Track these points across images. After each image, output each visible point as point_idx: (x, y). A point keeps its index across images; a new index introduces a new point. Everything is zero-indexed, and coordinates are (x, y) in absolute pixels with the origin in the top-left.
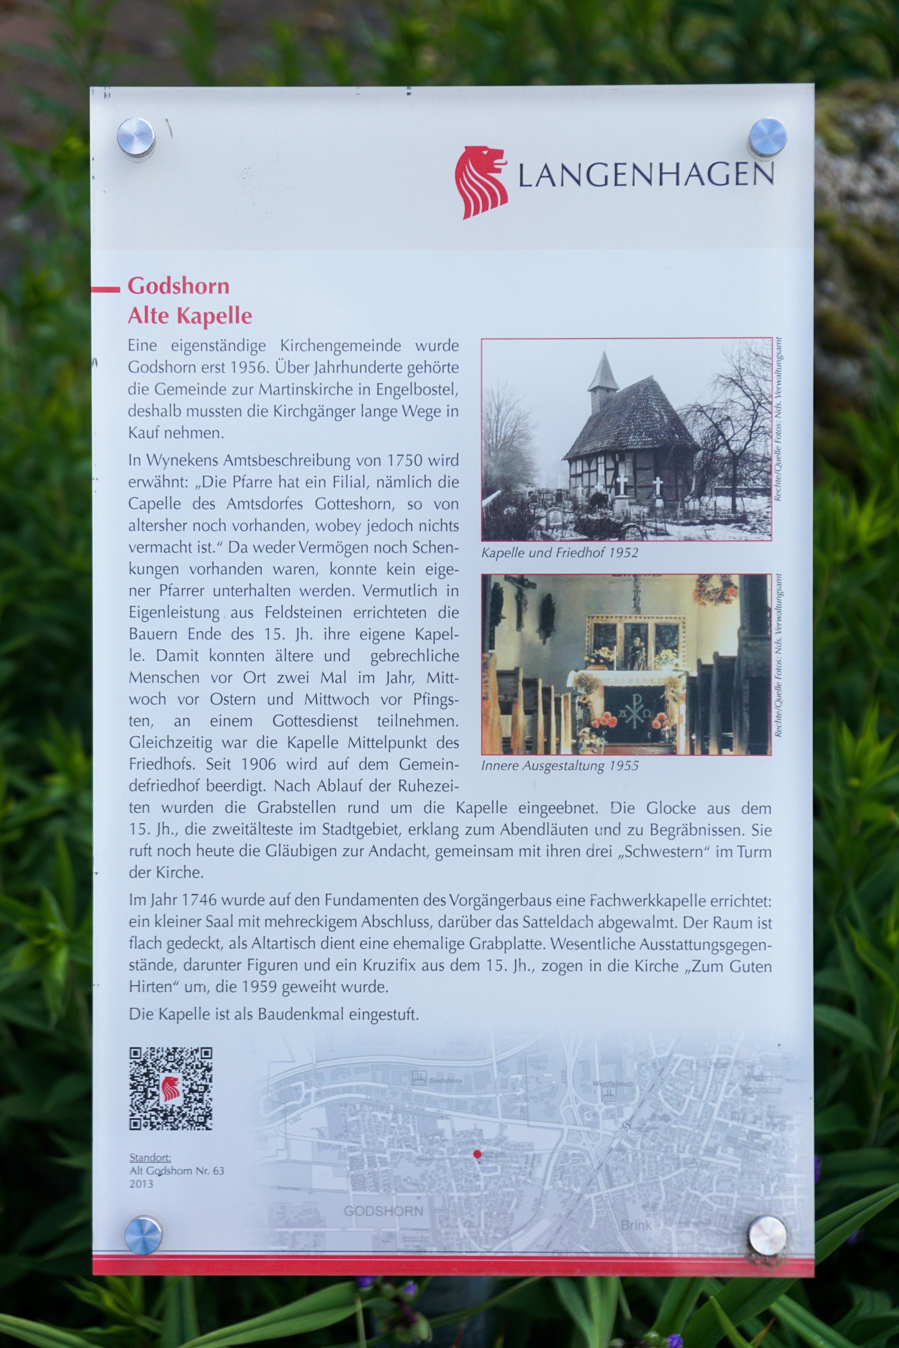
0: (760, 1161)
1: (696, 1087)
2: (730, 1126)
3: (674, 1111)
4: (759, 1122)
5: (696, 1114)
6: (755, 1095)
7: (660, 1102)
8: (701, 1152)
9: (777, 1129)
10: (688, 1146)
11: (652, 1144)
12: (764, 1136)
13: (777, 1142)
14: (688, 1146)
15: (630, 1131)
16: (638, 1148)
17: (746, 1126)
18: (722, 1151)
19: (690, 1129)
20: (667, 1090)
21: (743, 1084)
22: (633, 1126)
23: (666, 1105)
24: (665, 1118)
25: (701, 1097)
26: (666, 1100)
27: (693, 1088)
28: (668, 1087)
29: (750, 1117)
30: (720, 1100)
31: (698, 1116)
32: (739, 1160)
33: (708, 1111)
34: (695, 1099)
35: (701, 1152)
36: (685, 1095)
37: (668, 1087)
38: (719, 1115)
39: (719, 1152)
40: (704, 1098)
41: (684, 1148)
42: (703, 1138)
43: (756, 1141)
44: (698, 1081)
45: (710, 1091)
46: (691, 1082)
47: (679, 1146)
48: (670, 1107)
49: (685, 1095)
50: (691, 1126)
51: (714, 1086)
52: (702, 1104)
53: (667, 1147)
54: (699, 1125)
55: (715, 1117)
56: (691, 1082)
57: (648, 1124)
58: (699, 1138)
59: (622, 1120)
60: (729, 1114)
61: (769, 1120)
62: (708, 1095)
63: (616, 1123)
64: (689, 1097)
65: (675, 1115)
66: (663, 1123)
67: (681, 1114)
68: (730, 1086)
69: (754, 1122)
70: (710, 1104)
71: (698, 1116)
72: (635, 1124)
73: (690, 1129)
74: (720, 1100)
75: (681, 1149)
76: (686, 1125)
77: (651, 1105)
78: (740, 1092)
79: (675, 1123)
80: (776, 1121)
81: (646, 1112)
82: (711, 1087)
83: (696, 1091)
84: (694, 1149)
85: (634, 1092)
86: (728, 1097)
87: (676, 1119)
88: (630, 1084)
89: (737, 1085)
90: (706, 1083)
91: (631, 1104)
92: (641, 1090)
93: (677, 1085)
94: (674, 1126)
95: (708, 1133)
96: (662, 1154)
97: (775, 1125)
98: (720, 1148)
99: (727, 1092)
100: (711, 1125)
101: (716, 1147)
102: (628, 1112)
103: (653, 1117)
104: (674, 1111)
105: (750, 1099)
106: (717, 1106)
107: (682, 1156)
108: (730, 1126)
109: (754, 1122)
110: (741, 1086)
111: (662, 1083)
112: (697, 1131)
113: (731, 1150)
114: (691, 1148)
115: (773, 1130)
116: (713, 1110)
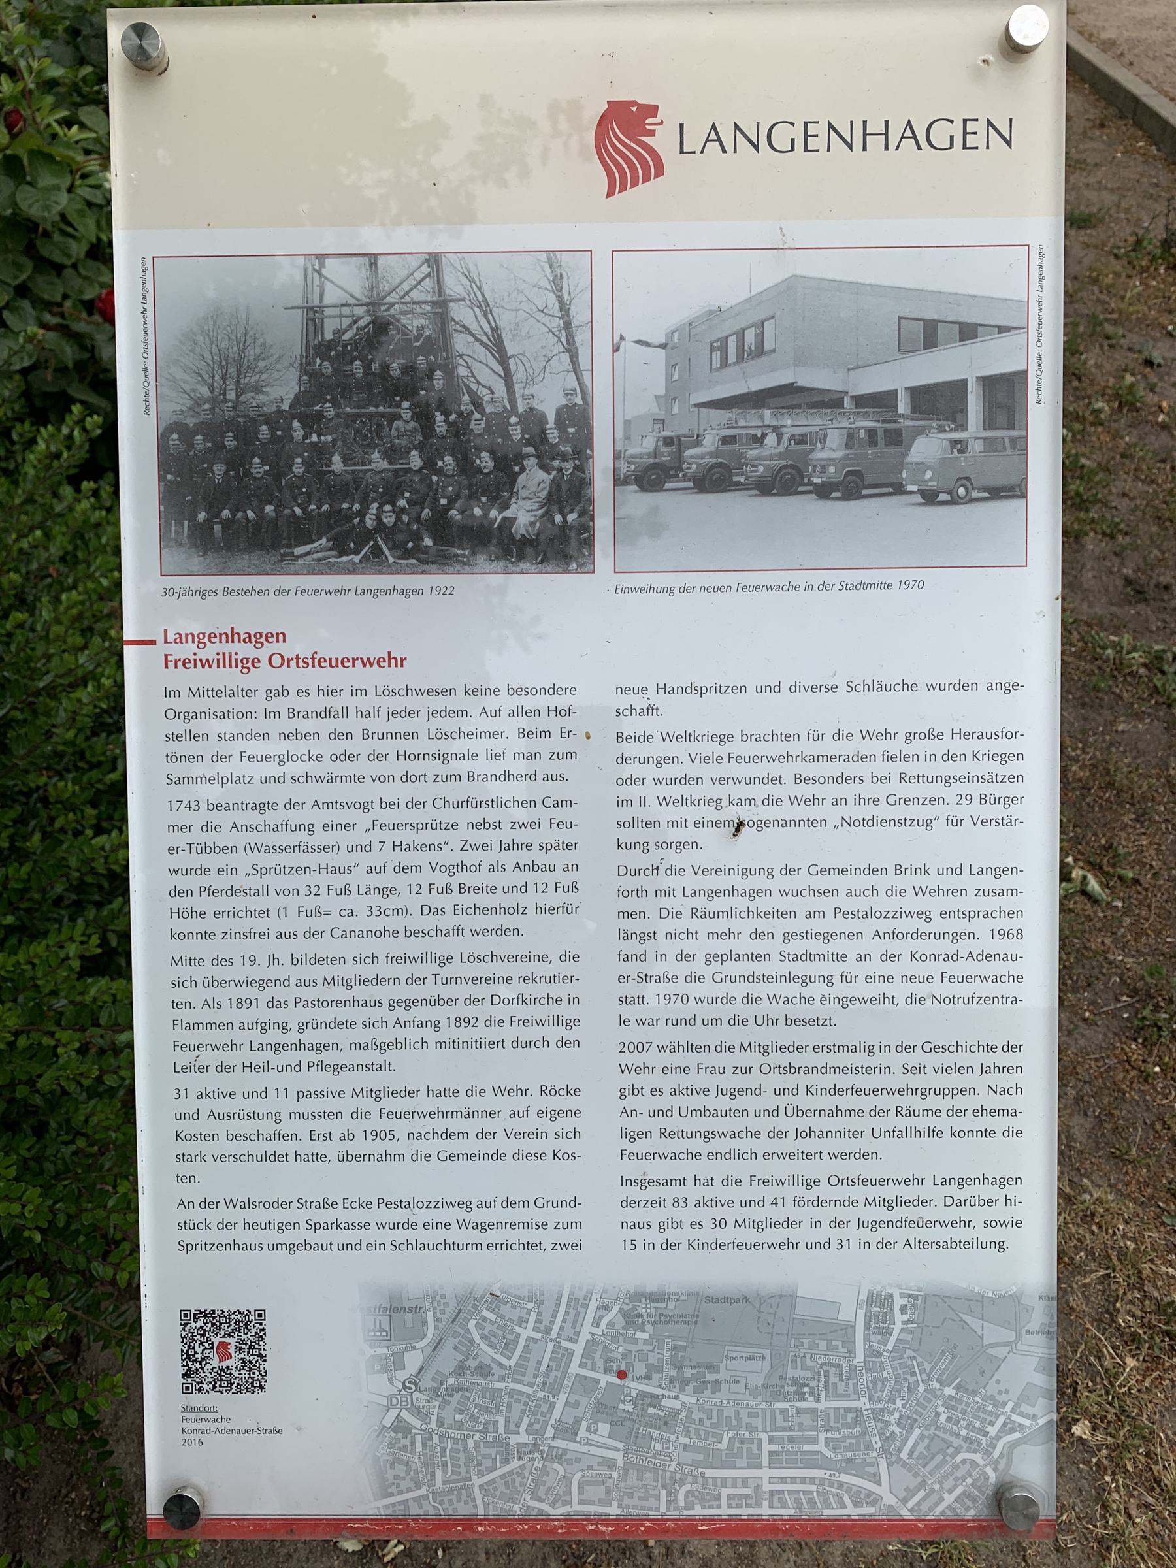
0: (658, 1447)
1: (539, 1314)
2: (603, 1384)
3: (499, 1358)
4: (656, 1376)
5: (540, 1362)
6: (648, 1327)
7: (472, 1341)
8: (550, 1432)
9: (689, 1389)
10: (526, 1421)
11: (459, 1418)
12: (665, 1402)
13: (689, 1413)
14: (526, 1421)
15: (416, 1395)
16: (433, 1424)
17: (632, 1384)
18: (588, 1430)
19: (530, 1390)
20: (485, 1319)
21: (626, 1308)
22: (422, 1386)
23: (483, 1346)
24: (483, 1371)
25: (548, 1331)
26: (484, 1337)
27: (533, 1315)
28: (486, 1313)
29: (639, 1369)
30: (584, 1336)
31: (543, 1367)
32: (620, 1445)
33: (562, 1357)
34: (538, 1336)
35: (550, 1432)
36: (518, 1329)
37: (486, 1313)
38: (582, 1365)
39: (582, 1432)
40: (554, 1335)
41: (518, 1425)
42: (552, 1406)
43: (651, 1410)
44: (542, 1302)
45: (564, 1321)
46: (530, 1305)
47: (507, 1421)
48: (491, 1351)
49: (518, 1329)
50: (530, 1385)
51: (572, 1312)
52: (550, 1346)
53: (486, 1423)
54: (545, 1384)
55: (574, 1369)
56: (530, 1305)
57: (451, 1381)
58: (545, 1408)
59: (402, 1375)
60: (600, 1363)
61: (674, 1373)
62: (562, 1328)
63: (391, 1380)
64: (526, 1332)
65: (501, 1365)
66: (477, 1379)
67: (512, 1362)
68: (601, 1312)
69: (648, 1377)
70: (564, 1344)
71: (543, 1367)
72: (426, 1382)
73: (530, 1390)
74: (584, 1336)
75: (512, 1427)
76: (522, 1382)
77: (455, 1348)
78: (621, 1322)
79: (501, 1379)
80: (688, 1373)
81: (448, 1359)
82: (567, 1313)
83: (538, 1321)
84: (537, 1427)
85: (425, 1323)
86: (599, 1331)
87: (502, 1372)
88: (418, 1310)
89: (616, 1309)
90: (558, 1306)
91: (418, 1345)
92: (437, 1319)
93: (505, 1310)
94: (498, 1385)
95: (563, 1398)
96: (477, 1437)
97: (686, 1382)
98: (584, 1424)
99: (597, 1323)
100: (568, 1383)
101: (578, 1422)
102: (413, 1361)
103: (460, 1369)
104: (499, 1358)
105: (639, 1335)
106: (578, 1348)
107: (514, 1439)
108: (603, 1384)
109: (648, 1377)
110: (621, 1309)
111: (475, 1307)
112: (541, 1394)
113: (604, 1428)
114: (530, 1424)
115: (682, 1391)
116: (571, 1354)
